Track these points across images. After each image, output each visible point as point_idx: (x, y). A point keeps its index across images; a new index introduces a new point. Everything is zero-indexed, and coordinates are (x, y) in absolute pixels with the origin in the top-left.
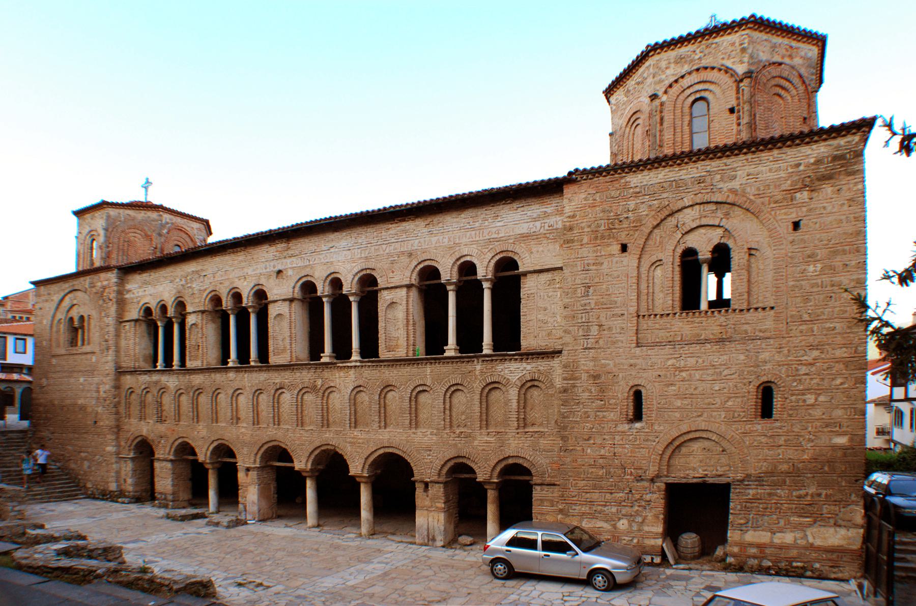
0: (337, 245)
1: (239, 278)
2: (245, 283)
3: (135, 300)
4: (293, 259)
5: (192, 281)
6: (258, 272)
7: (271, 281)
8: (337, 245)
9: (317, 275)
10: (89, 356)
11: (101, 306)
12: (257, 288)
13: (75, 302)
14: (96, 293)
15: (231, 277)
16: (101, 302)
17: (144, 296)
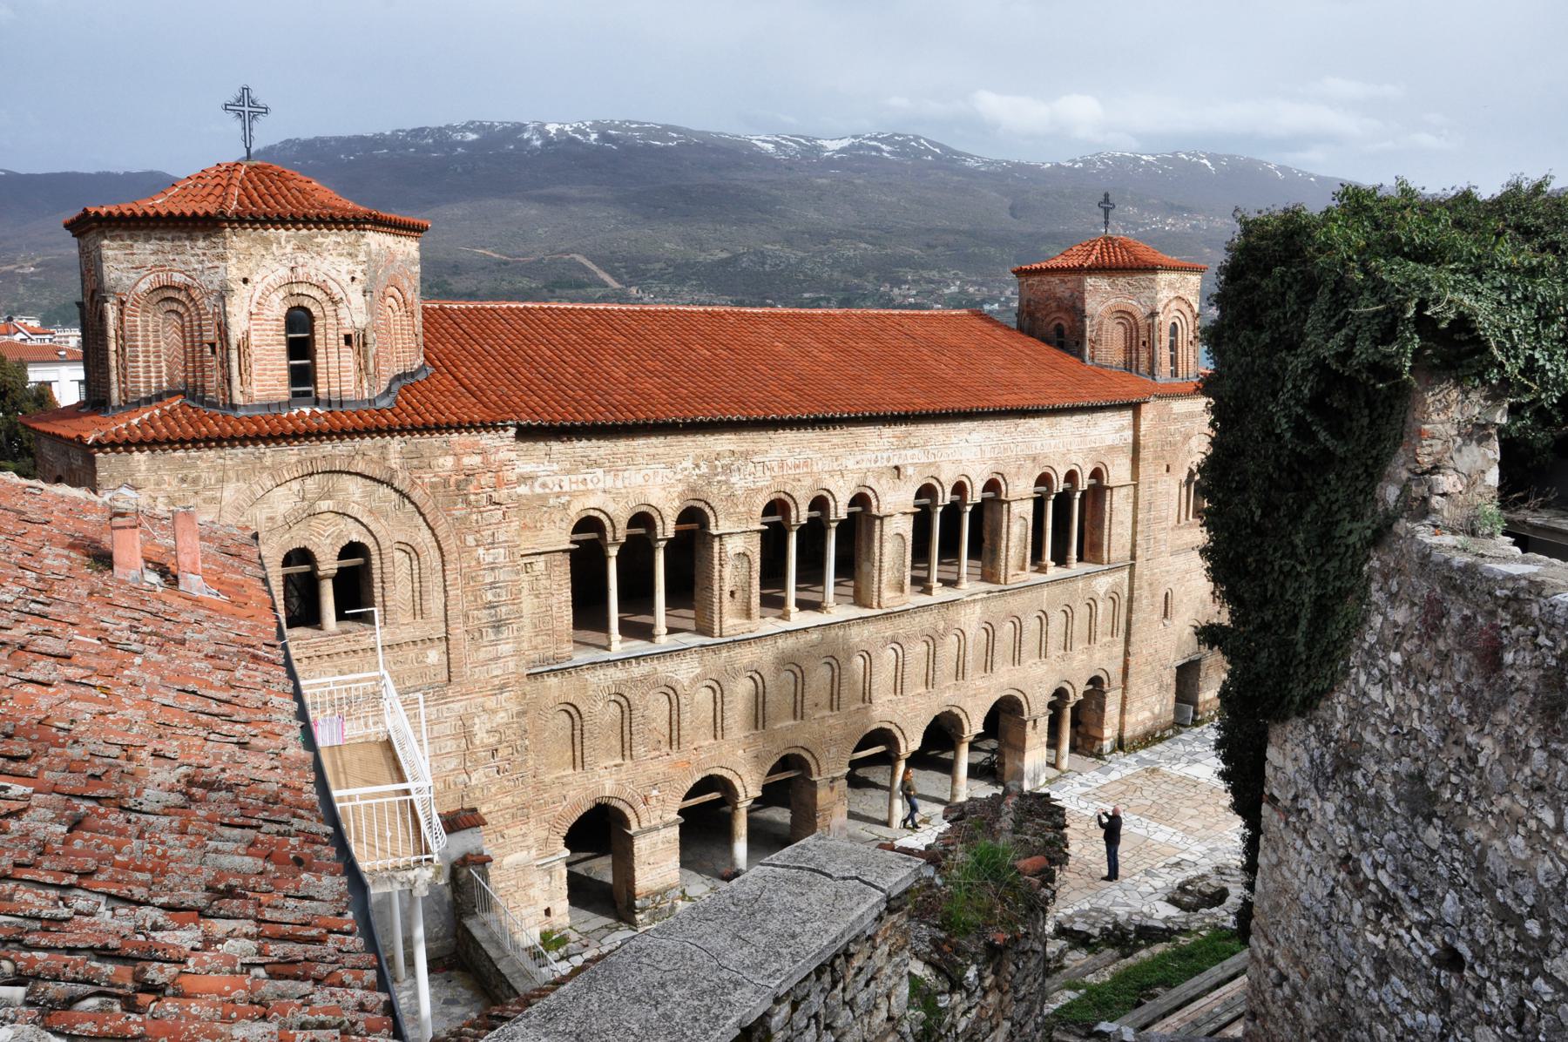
0: (969, 438)
1: (831, 473)
2: (841, 483)
3: (552, 502)
4: (915, 451)
5: (728, 469)
6: (864, 465)
7: (883, 481)
8: (969, 438)
9: (942, 479)
10: (411, 653)
11: (463, 520)
12: (857, 491)
13: (324, 505)
14: (433, 486)
15: (815, 469)
16: (459, 511)
17: (584, 493)
